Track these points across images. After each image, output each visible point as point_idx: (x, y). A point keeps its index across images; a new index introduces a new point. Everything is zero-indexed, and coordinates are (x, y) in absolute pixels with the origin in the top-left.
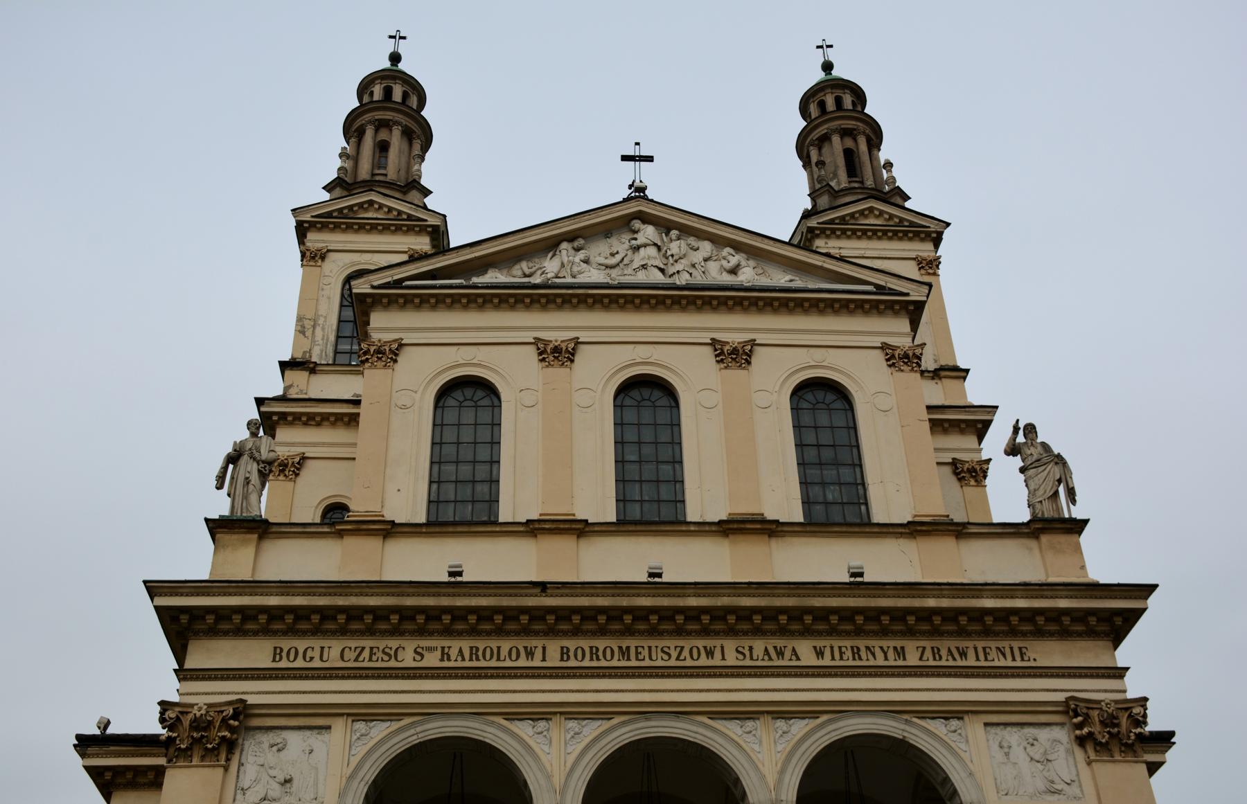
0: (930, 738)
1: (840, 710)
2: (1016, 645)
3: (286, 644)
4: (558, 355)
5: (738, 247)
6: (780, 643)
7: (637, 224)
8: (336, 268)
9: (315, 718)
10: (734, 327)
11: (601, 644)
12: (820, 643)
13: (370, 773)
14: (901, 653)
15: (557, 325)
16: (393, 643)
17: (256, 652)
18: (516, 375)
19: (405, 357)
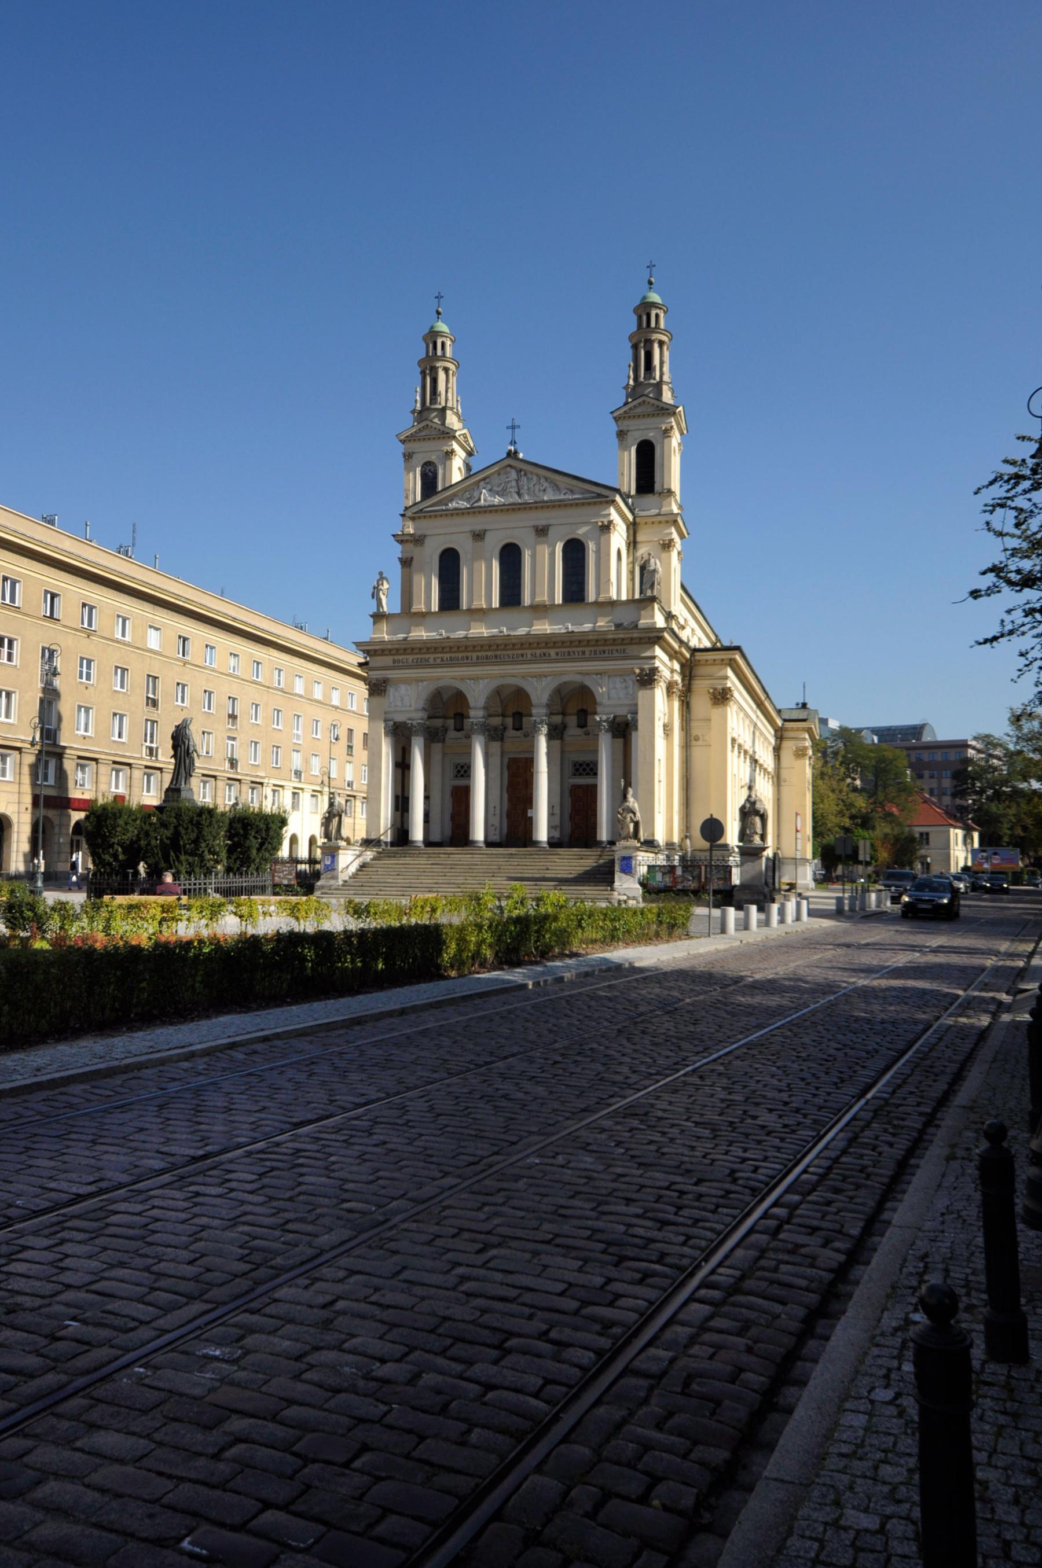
0: (588, 682)
1: (562, 674)
2: (623, 647)
3: (396, 657)
4: (478, 536)
5: (546, 479)
6: (544, 651)
7: (508, 469)
8: (420, 459)
9: (407, 681)
10: (541, 518)
11: (489, 654)
12: (557, 650)
13: (424, 695)
14: (584, 653)
15: (477, 523)
16: (427, 656)
17: (388, 660)
18: (464, 547)
19: (427, 541)
